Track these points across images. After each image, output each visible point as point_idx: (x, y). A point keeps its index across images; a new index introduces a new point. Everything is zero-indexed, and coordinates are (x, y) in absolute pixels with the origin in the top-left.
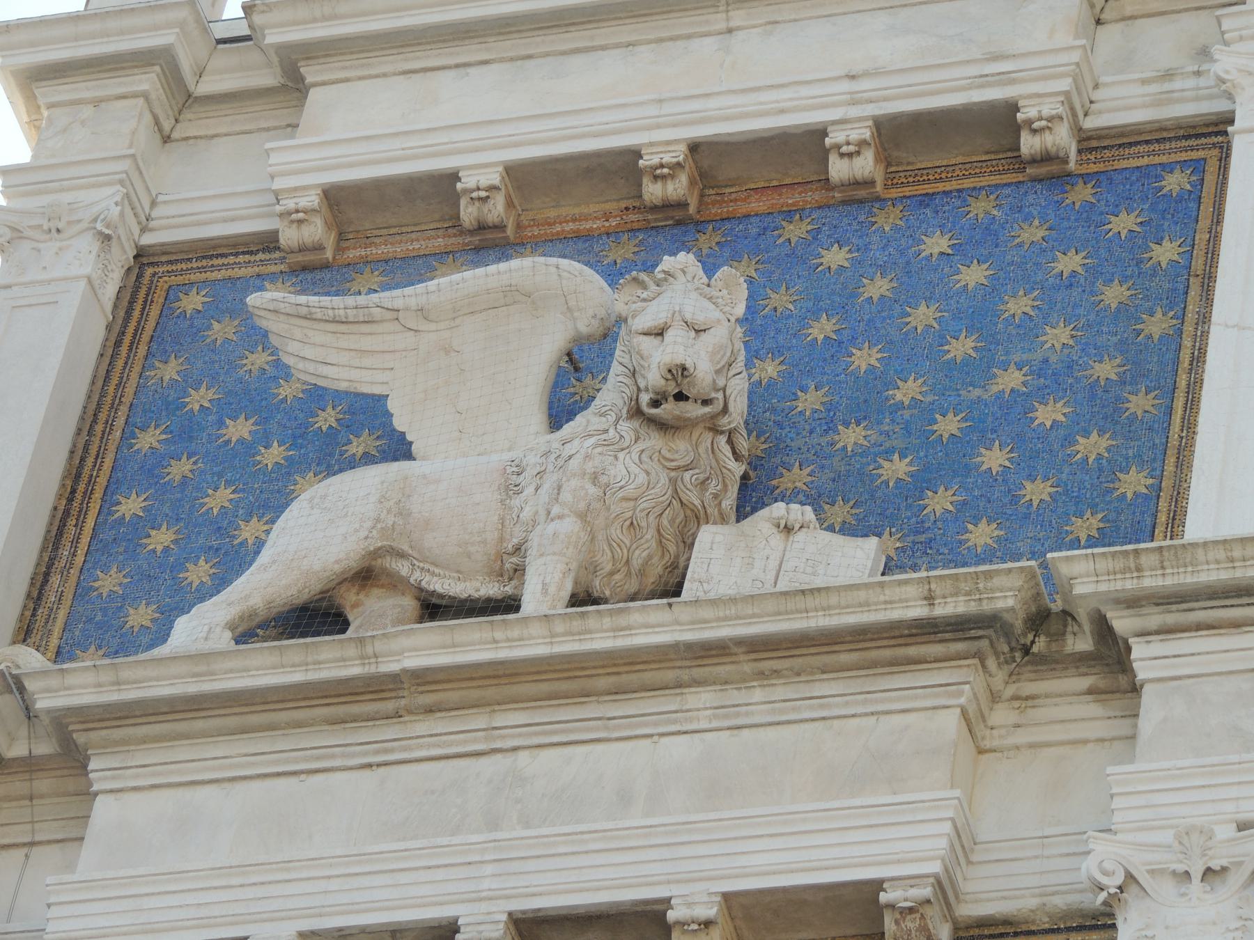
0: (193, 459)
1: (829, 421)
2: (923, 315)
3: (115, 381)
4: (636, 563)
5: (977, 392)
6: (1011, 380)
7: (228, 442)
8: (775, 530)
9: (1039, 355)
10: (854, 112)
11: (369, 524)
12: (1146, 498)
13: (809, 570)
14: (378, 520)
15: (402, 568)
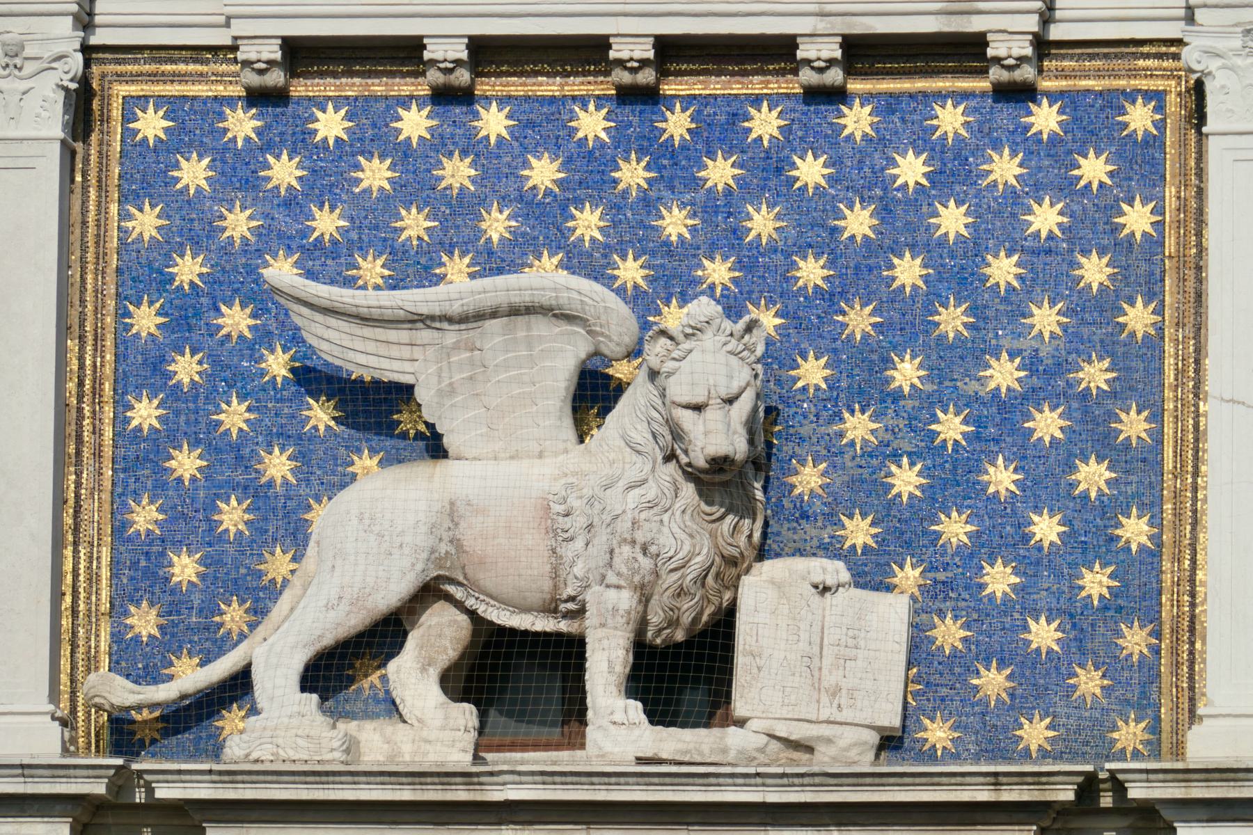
0: (198, 357)
1: (832, 403)
2: (908, 271)
3: (92, 230)
4: (686, 619)
5: (974, 386)
6: (1003, 374)
7: (228, 336)
8: (813, 590)
9: (1026, 344)
10: (822, 25)
11: (425, 555)
12: (1152, 554)
13: (851, 642)
14: (433, 552)
15: (458, 593)
